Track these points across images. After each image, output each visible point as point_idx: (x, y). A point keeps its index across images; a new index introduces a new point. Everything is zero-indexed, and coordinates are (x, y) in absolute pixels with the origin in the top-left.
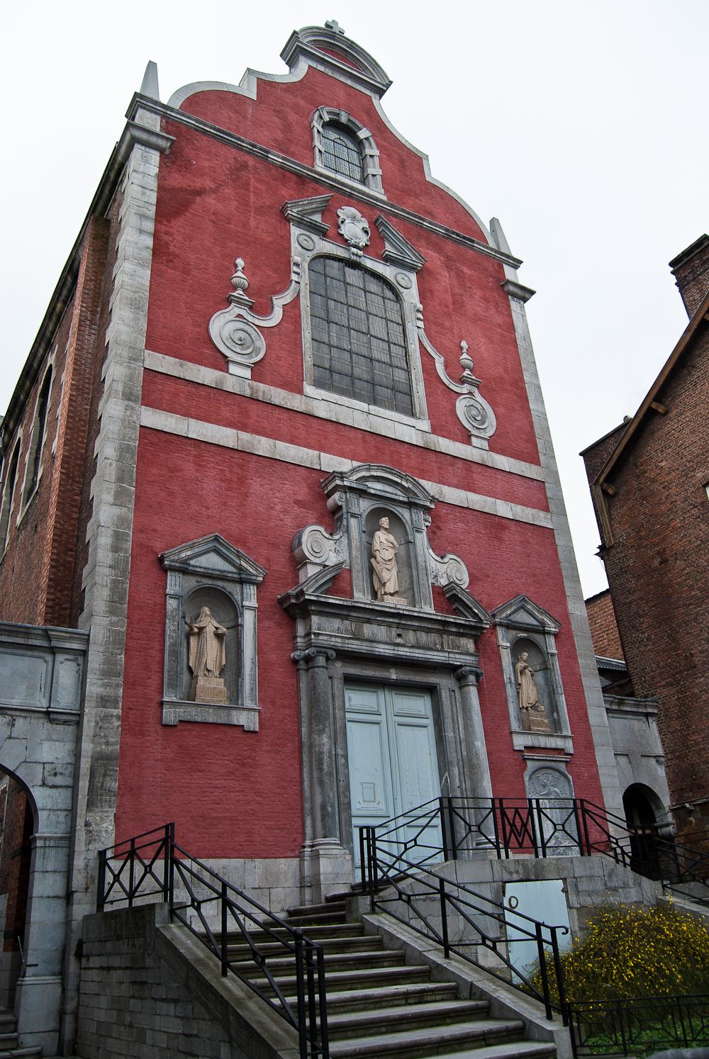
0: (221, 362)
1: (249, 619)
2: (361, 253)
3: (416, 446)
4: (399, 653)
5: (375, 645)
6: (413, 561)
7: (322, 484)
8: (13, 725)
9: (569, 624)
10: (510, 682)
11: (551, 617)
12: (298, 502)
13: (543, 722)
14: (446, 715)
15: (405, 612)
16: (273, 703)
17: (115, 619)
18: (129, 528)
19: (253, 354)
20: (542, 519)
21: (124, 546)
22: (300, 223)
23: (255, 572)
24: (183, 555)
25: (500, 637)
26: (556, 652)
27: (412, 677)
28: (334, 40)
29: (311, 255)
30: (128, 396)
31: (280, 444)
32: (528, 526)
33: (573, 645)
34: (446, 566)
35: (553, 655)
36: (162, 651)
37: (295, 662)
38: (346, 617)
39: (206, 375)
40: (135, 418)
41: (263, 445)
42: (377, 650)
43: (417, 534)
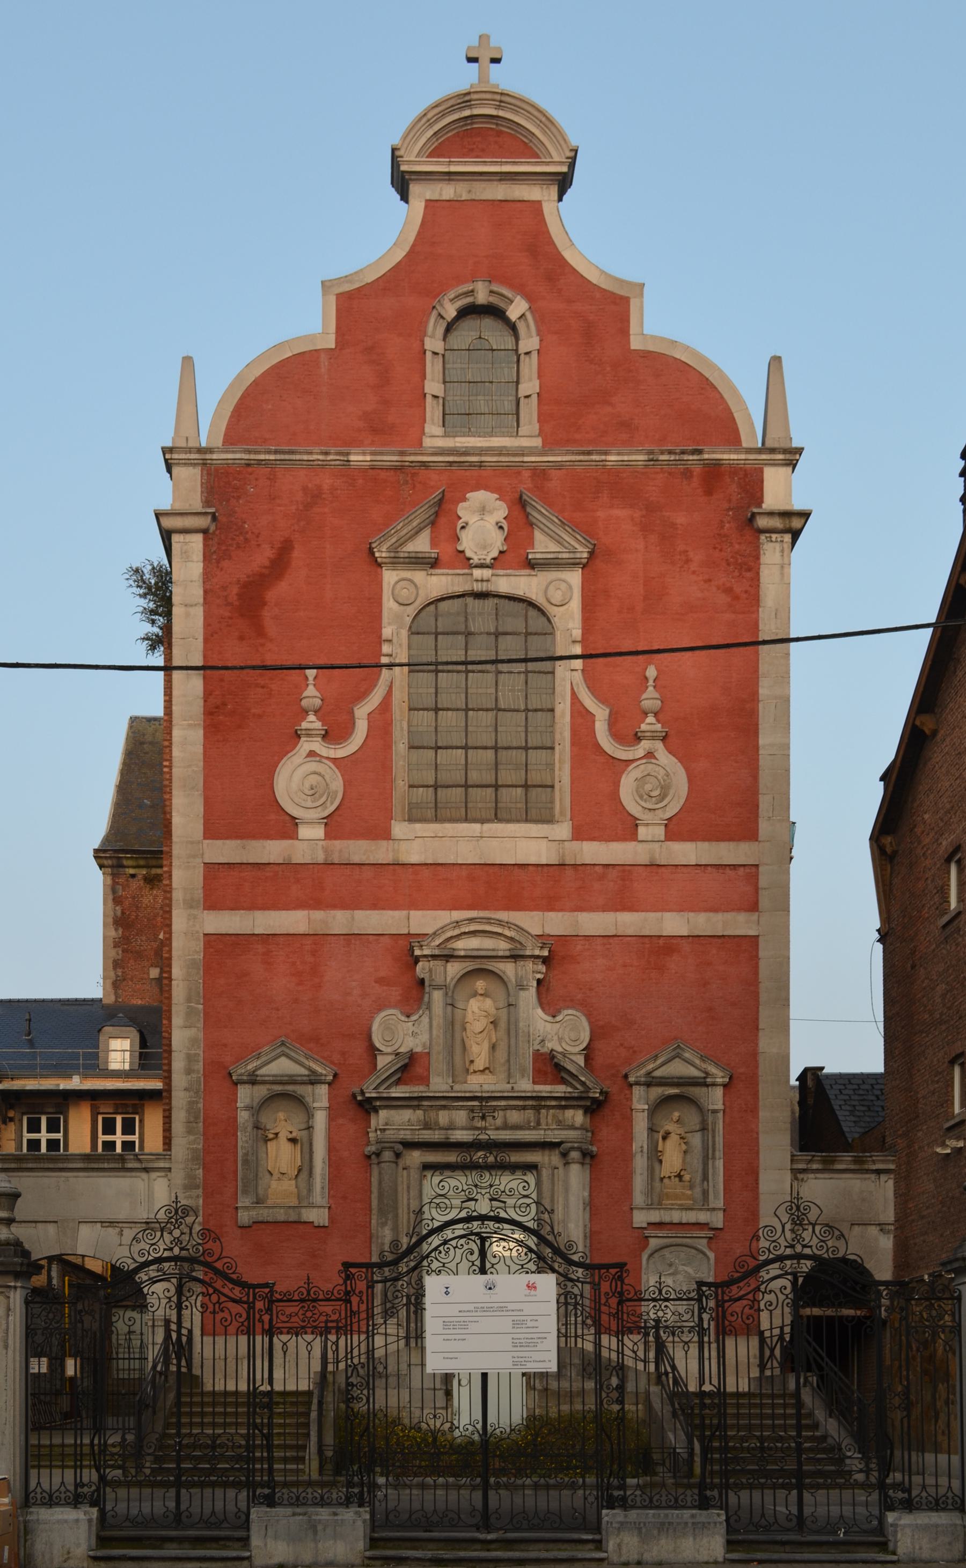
0: (288, 827)
1: (320, 1120)
2: (487, 573)
3: (547, 865)
5: (450, 1132)
6: (512, 1027)
7: (406, 951)
8: (122, 1235)
9: (757, 1067)
10: (642, 1151)
11: (717, 1065)
12: (380, 981)
13: (683, 1194)
17: (192, 1138)
18: (199, 1047)
19: (328, 803)
21: (196, 1067)
22: (396, 562)
23: (324, 1072)
28: (470, 107)
29: (412, 610)
30: (189, 904)
31: (359, 914)
33: (756, 1095)
34: (558, 1025)
35: (715, 1112)
36: (236, 1161)
37: (369, 1157)
38: (418, 1107)
39: (271, 851)
41: (339, 921)
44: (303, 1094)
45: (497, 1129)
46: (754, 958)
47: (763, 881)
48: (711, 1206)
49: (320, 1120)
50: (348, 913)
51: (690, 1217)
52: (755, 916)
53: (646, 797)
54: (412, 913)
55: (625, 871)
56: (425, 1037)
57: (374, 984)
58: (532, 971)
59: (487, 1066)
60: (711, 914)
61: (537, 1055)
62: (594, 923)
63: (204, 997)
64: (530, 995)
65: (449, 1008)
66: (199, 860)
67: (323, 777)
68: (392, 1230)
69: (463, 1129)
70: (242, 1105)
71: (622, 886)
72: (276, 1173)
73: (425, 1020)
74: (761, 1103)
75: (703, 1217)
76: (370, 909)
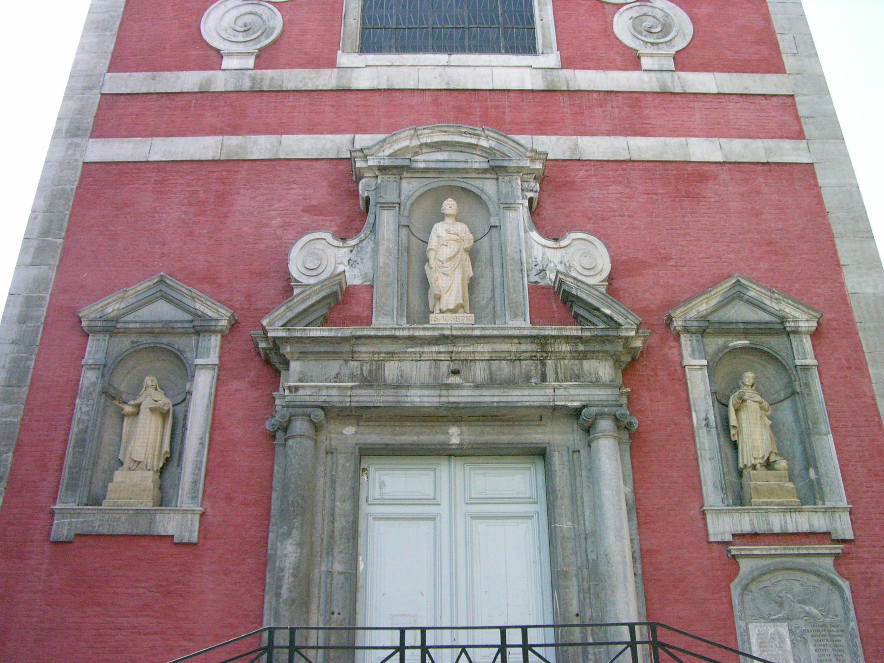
0: (211, 58)
1: (203, 385)
4: (452, 399)
5: (403, 392)
9: (849, 311)
10: (707, 425)
12: (310, 210)
13: (782, 488)
14: (559, 494)
15: (455, 333)
16: (229, 499)
20: (787, 151)
23: (215, 316)
24: (109, 310)
25: (686, 349)
26: (814, 362)
27: (493, 434)
32: (759, 168)
33: (857, 347)
35: (805, 368)
36: (66, 442)
39: (188, 80)
40: (78, 156)
41: (260, 146)
42: (409, 399)
43: (508, 213)
44: (182, 347)
45: (477, 386)
46: (814, 187)
47: (802, 111)
48: (828, 504)
49: (203, 385)
50: (274, 138)
51: (801, 522)
52: (803, 144)
53: (645, 33)
54: (358, 136)
55: (635, 98)
56: (366, 266)
57: (301, 214)
58: (522, 191)
59: (461, 301)
60: (748, 141)
61: (534, 288)
62: (598, 147)
63: (68, 231)
64: (521, 215)
65: (404, 231)
66: (98, 92)
67: (260, 16)
68: (300, 545)
69: (423, 386)
70: (90, 362)
71: (632, 113)
72: (127, 463)
73: (368, 245)
74: (867, 358)
75: (819, 523)
76: (305, 133)
